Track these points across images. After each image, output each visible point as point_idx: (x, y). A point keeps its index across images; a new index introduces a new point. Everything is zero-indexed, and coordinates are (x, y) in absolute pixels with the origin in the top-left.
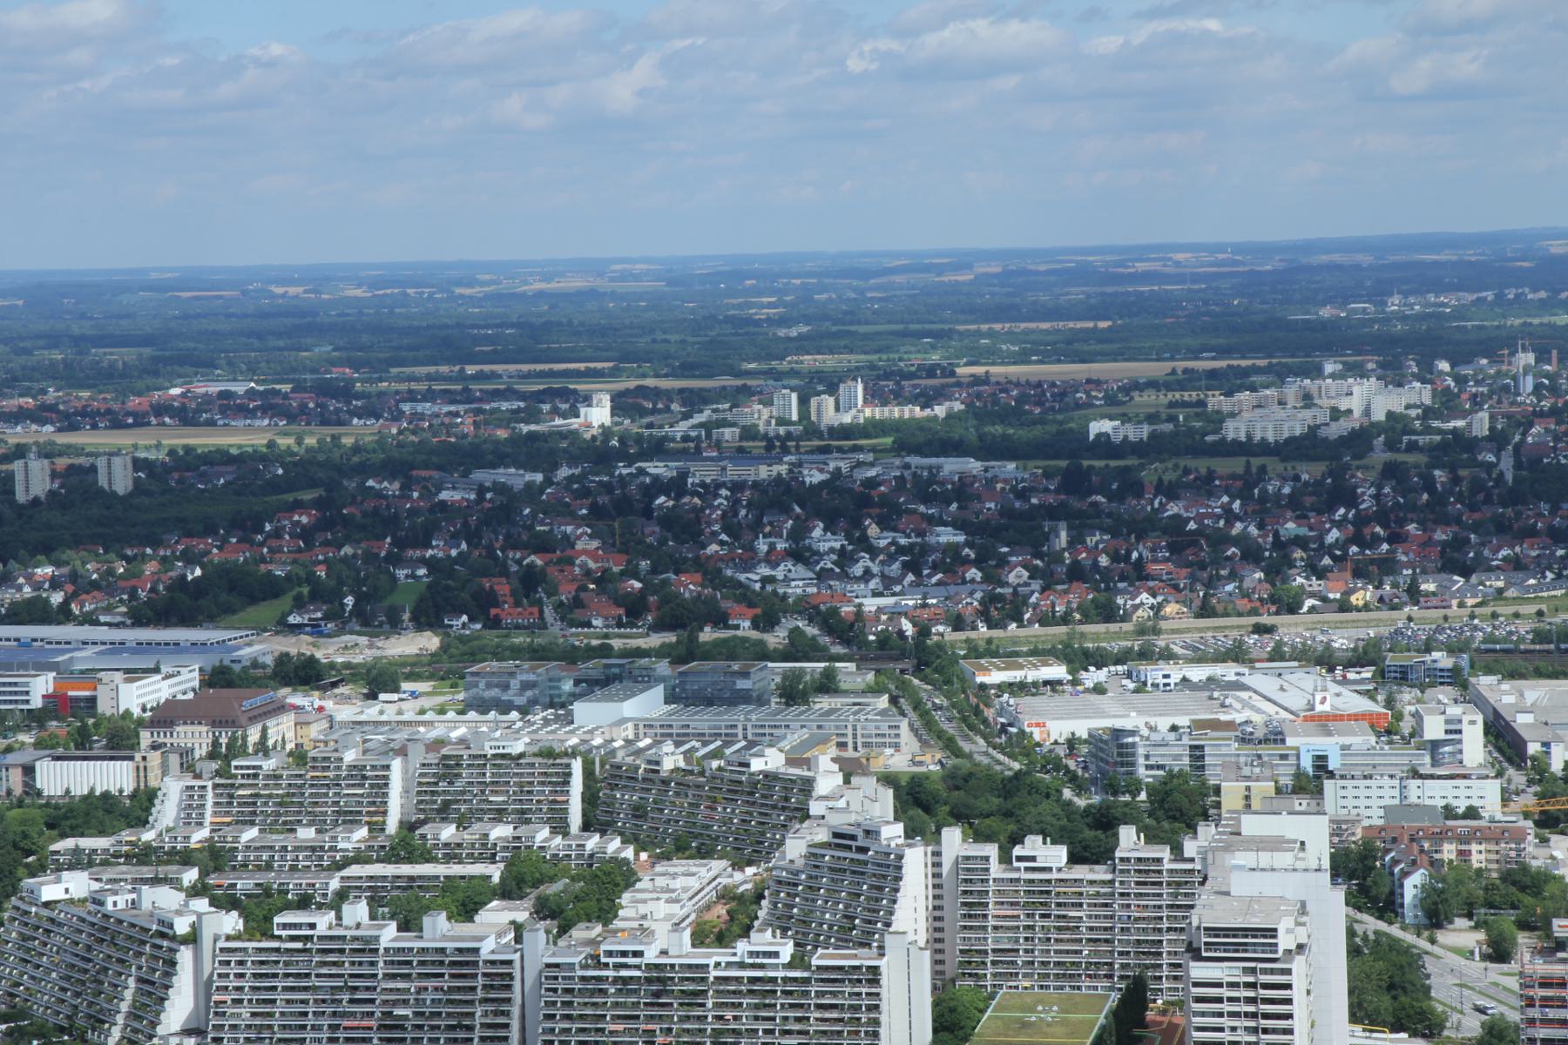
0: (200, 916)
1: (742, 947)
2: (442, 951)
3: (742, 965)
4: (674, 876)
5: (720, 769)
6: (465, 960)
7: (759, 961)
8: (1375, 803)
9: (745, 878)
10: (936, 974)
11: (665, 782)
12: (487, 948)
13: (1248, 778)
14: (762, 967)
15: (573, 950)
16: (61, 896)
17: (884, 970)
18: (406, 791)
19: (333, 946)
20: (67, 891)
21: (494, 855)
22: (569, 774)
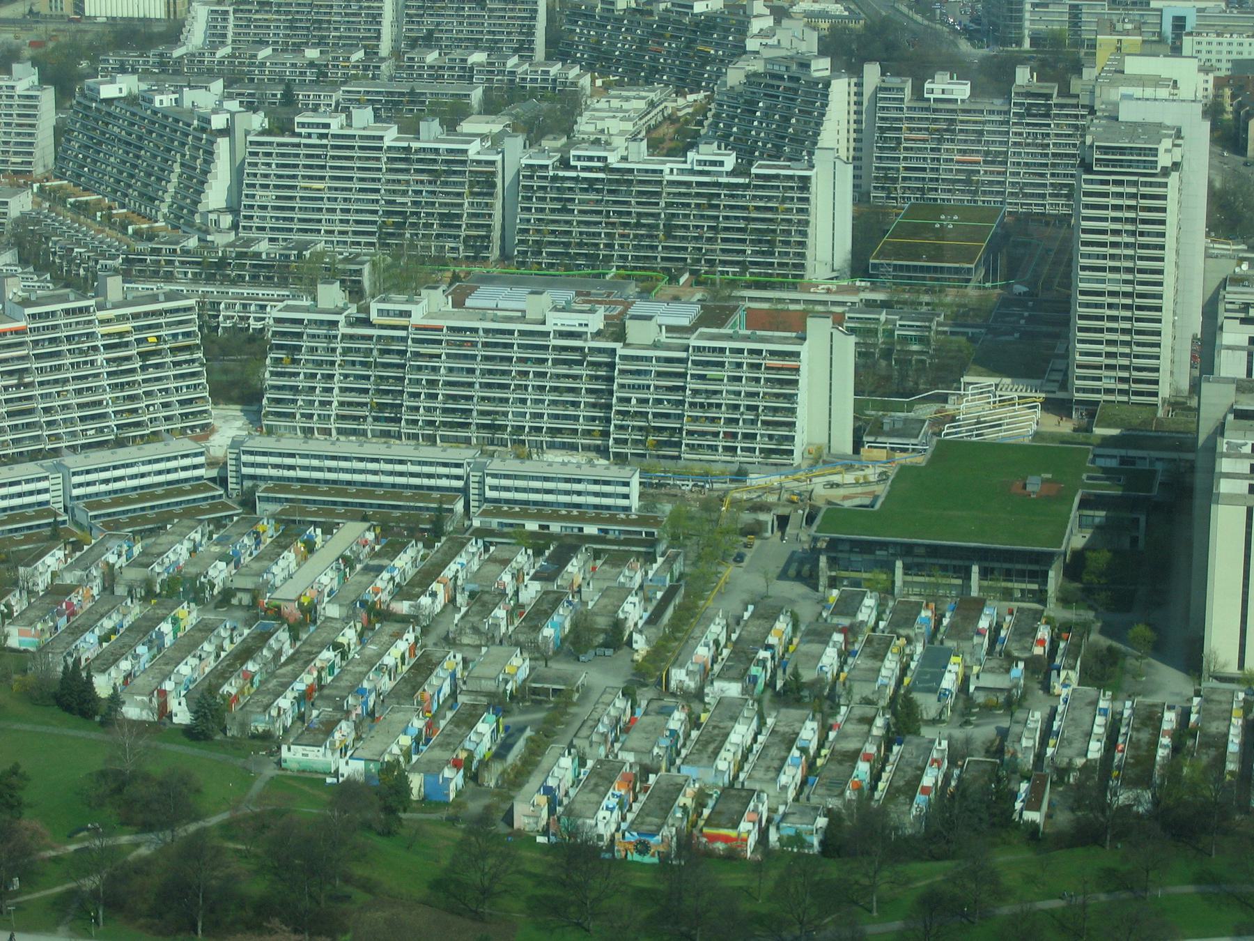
0: (233, 114)
1: (691, 155)
2: (436, 151)
3: (692, 172)
4: (627, 99)
5: (666, 10)
6: (457, 160)
7: (706, 168)
8: (1224, 57)
9: (686, 103)
10: (856, 187)
11: (619, 20)
12: (474, 150)
13: (1120, 33)
14: (707, 173)
15: (546, 155)
16: (116, 94)
17: (813, 180)
18: (397, 22)
19: (344, 142)
20: (121, 90)
21: (472, 77)
22: (536, 11)
